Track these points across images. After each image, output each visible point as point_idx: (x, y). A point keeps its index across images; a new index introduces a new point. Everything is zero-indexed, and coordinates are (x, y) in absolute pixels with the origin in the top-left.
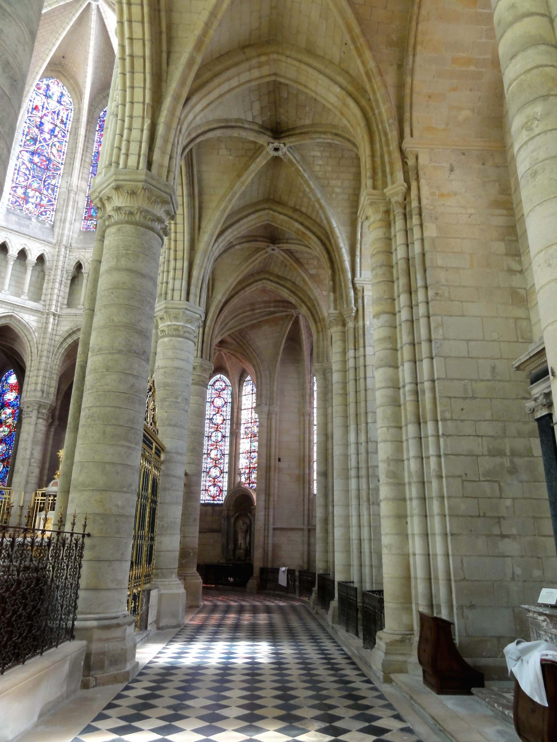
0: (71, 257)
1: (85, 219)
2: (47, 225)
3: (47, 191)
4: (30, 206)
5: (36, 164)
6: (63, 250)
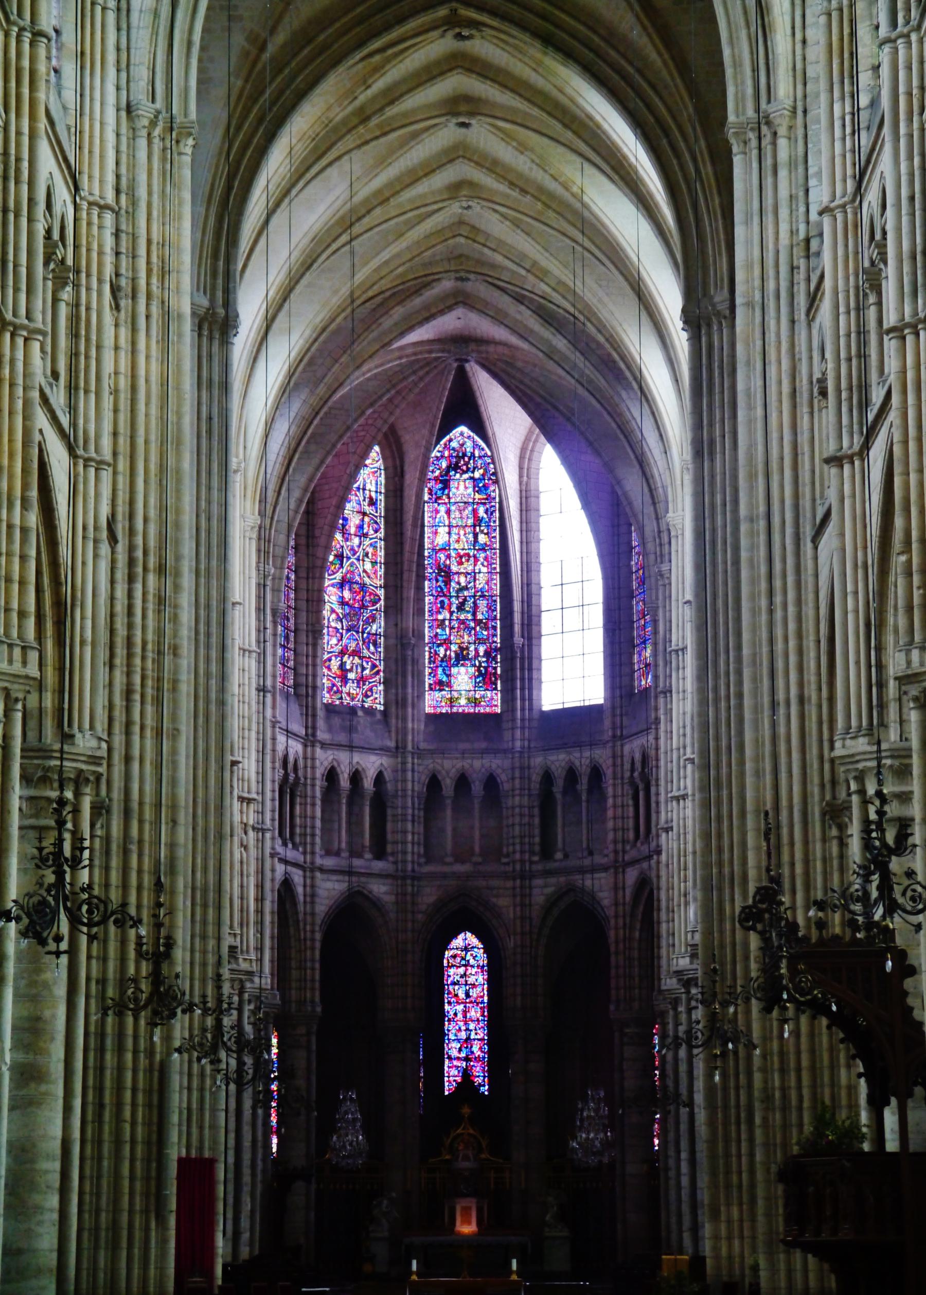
0: (421, 769)
1: (431, 689)
2: (379, 716)
3: (368, 649)
4: (351, 687)
5: (347, 604)
6: (410, 760)
